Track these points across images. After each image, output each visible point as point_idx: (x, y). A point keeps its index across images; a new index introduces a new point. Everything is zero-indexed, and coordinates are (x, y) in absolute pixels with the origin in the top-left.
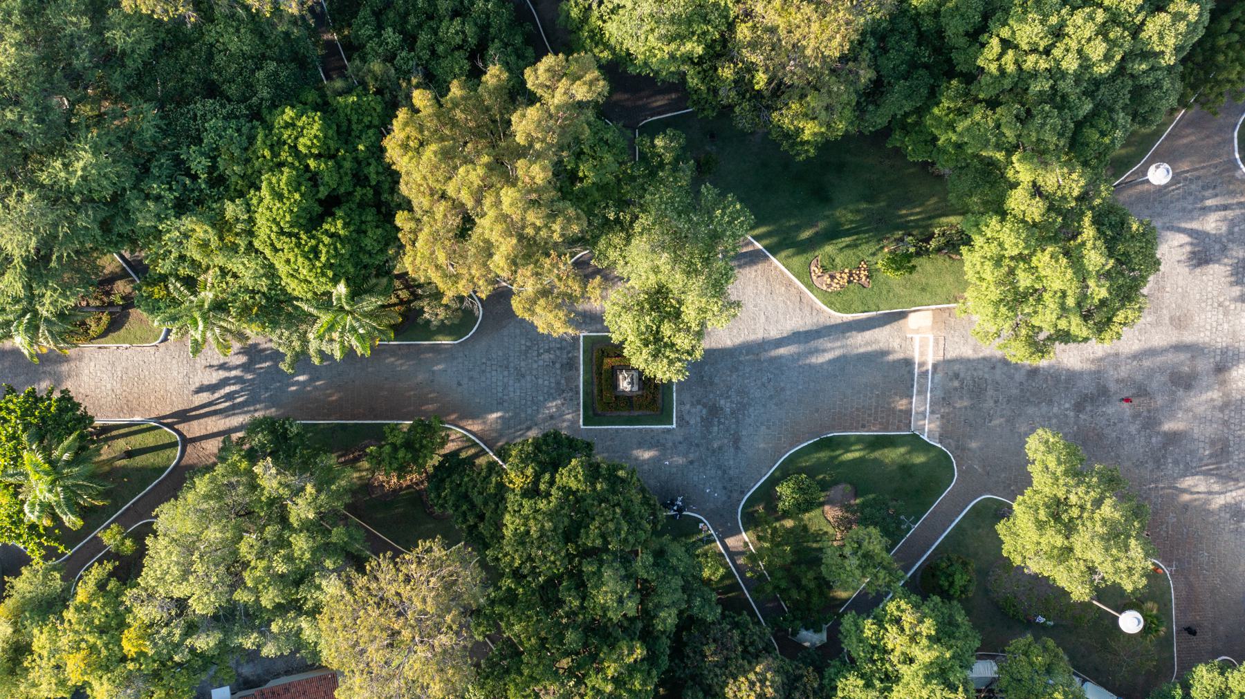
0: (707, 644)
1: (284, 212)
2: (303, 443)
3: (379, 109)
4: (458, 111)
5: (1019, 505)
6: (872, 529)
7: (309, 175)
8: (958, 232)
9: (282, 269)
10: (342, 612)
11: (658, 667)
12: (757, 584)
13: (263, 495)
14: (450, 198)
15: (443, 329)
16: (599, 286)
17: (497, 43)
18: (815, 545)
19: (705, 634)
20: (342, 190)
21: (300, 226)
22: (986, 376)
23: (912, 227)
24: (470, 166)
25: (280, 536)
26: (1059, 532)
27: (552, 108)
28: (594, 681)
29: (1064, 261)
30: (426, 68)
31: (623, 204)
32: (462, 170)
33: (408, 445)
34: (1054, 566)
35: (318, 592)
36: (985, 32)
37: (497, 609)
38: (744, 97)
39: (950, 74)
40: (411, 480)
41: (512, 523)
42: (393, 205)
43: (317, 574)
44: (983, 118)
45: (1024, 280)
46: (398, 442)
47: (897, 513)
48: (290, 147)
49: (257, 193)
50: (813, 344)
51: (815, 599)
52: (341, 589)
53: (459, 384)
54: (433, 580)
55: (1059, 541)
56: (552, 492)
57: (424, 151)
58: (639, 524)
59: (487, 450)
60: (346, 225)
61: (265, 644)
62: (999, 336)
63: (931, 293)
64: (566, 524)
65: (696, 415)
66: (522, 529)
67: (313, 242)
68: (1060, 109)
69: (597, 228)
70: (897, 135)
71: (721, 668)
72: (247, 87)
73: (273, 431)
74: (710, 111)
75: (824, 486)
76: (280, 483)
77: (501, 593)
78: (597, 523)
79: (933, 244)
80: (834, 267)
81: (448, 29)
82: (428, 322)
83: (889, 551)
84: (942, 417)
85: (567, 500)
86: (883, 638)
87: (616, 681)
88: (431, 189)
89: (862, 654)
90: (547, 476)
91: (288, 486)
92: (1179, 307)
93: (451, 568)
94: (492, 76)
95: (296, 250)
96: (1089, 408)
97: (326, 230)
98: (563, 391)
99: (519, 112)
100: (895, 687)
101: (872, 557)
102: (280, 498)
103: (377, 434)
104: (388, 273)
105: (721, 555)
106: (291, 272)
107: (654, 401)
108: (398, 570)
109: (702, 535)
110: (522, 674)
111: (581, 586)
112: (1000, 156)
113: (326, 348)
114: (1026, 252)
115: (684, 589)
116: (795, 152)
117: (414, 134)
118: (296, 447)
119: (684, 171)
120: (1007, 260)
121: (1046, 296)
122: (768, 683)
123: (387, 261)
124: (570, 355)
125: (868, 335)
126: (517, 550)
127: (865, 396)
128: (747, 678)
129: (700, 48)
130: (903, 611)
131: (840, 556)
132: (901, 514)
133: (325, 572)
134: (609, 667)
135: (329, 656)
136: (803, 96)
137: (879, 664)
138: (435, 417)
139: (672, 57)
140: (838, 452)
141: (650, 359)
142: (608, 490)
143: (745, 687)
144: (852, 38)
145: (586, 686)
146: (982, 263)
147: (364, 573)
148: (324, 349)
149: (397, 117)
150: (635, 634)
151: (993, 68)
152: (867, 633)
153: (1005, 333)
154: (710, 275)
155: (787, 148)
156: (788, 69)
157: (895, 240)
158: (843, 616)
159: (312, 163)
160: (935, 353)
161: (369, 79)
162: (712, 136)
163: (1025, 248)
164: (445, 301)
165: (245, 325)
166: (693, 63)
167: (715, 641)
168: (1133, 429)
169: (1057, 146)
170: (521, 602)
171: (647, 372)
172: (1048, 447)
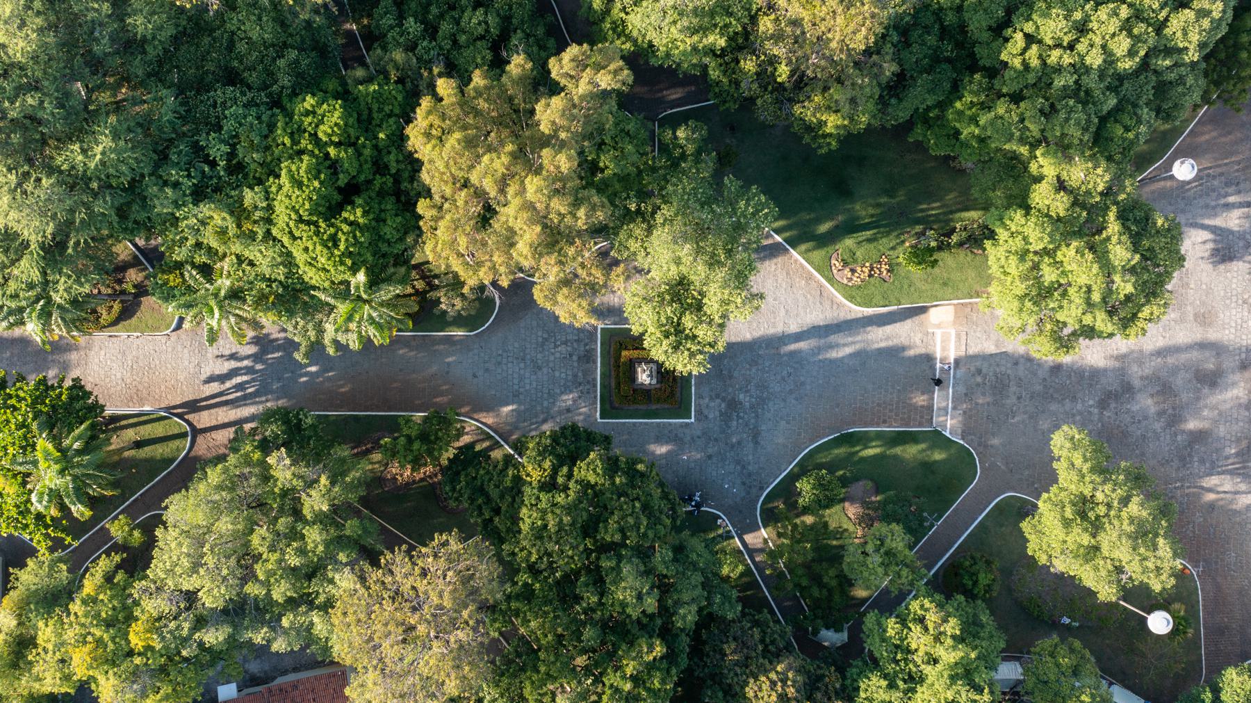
0: (727, 642)
1: (304, 199)
2: (316, 434)
3: (400, 98)
4: (481, 101)
5: (1045, 502)
6: (894, 526)
7: (329, 162)
8: (979, 226)
9: (300, 257)
10: (356, 608)
11: (677, 665)
12: (776, 580)
13: (276, 486)
14: (473, 185)
15: (459, 321)
16: (623, 274)
17: (519, 34)
18: (835, 543)
19: (725, 632)
20: (362, 178)
21: (320, 214)
22: (1009, 372)
23: (933, 222)
24: (494, 155)
25: (293, 528)
26: (1086, 530)
27: (575, 97)
28: (612, 679)
29: (1089, 256)
30: (447, 58)
31: (643, 195)
32: (486, 159)
33: (424, 437)
34: (1081, 565)
35: (330, 586)
36: (1009, 27)
37: (514, 605)
38: (766, 90)
39: (973, 67)
40: (425, 473)
41: (530, 517)
42: (412, 193)
43: (330, 567)
44: (1006, 112)
45: (1049, 275)
46: (413, 434)
47: (920, 510)
48: (310, 135)
49: (277, 181)
50: (833, 338)
51: (837, 598)
52: (355, 583)
53: (475, 376)
54: (450, 574)
55: (1086, 540)
56: (570, 486)
57: (447, 140)
58: (659, 519)
59: (502, 443)
60: (365, 213)
61: (275, 639)
62: (1024, 331)
63: (953, 288)
64: (585, 518)
65: (714, 409)
66: (539, 523)
67: (332, 230)
68: (1085, 103)
69: (618, 219)
70: (919, 129)
71: (741, 667)
72: (268, 75)
73: (286, 422)
74: (731, 104)
75: (844, 482)
76: (294, 474)
77: (517, 588)
78: (616, 518)
79: (955, 239)
80: (855, 261)
81: (470, 19)
82: (445, 313)
83: (911, 548)
84: (965, 412)
85: (585, 493)
86: (907, 638)
87: (635, 679)
88: (454, 178)
89: (885, 654)
90: (565, 470)
91: (301, 477)
92: (1203, 303)
93: (468, 563)
94: (517, 66)
95: (314, 238)
96: (1113, 405)
97: (345, 218)
98: (580, 384)
99: (543, 101)
100: (919, 688)
101: (894, 555)
102: (294, 489)
103: (392, 426)
104: (406, 262)
105: (740, 552)
106: (309, 260)
107: (672, 394)
108: (414, 564)
109: (720, 531)
110: (538, 672)
111: (599, 582)
112: (1024, 150)
113: (341, 338)
114: (1051, 246)
115: (704, 586)
116: (816, 145)
117: (437, 122)
118: (310, 438)
119: (706, 163)
120: (1031, 255)
121: (1071, 291)
122: (789, 683)
123: (406, 250)
124: (587, 347)
125: (888, 329)
126: (535, 545)
127: (886, 391)
128: (768, 678)
129: (723, 40)
130: (927, 610)
131: (862, 553)
132: (923, 511)
133: (338, 566)
134: (627, 665)
135: (340, 651)
136: (826, 89)
137: (902, 664)
138: (451, 409)
139: (695, 49)
140: (858, 448)
141: (670, 351)
142: (627, 484)
143: (766, 686)
144: (877, 31)
145: (604, 685)
146: (1007, 258)
147: (379, 567)
148: (339, 339)
149: (420, 105)
150: (654, 631)
151: (1017, 63)
152: (891, 632)
153: (1029, 328)
154: (734, 267)
155: (808, 141)
156: (810, 62)
157: (916, 233)
158: (865, 615)
159: (332, 151)
160: (957, 348)
161: (390, 68)
162: (732, 129)
163: (1050, 242)
164: (466, 290)
165: (261, 314)
166: (715, 55)
167: (735, 639)
168: (1158, 426)
169: (1081, 140)
170: (538, 597)
171: (667, 364)
172: (1074, 443)
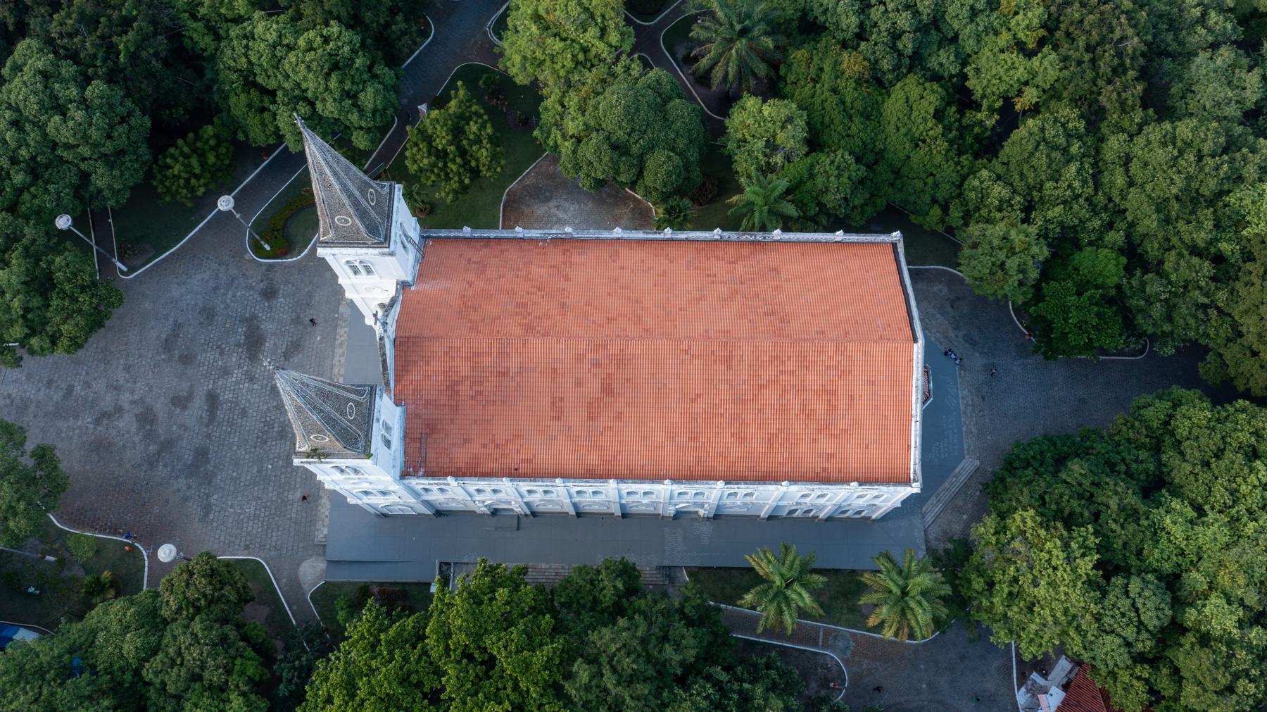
168: (137, 439)
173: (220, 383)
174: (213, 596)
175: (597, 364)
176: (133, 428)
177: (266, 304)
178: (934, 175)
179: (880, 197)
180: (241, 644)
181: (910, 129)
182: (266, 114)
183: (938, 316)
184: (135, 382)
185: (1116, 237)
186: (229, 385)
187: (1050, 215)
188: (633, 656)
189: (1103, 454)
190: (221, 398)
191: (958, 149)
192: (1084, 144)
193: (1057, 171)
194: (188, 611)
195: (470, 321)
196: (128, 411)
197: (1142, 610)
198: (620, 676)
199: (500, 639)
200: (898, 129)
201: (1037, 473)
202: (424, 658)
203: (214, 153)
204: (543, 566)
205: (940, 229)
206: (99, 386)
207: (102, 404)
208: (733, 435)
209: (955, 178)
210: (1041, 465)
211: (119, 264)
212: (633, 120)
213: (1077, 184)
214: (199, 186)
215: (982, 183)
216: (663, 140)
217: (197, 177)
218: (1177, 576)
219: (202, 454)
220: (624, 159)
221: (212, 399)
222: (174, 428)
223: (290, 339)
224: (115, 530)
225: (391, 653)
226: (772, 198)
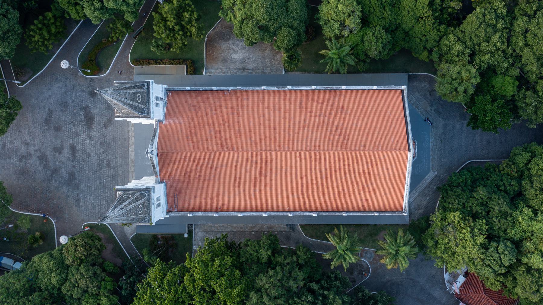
96: (24, 161)
168: (40, 168)
173: (75, 140)
174: (87, 254)
175: (256, 163)
176: (38, 163)
177: (92, 100)
178: (426, 36)
179: (398, 46)
180: (103, 275)
181: (415, 12)
182: (78, 7)
183: (423, 99)
184: (34, 141)
185: (515, 72)
186: (80, 141)
187: (483, 59)
188: (276, 288)
189: (495, 181)
190: (77, 148)
191: (439, 22)
192: (505, 21)
193: (489, 37)
194: (77, 261)
195: (193, 142)
196: (34, 155)
197: (503, 259)
198: (271, 297)
199: (217, 283)
200: (409, 12)
201: (463, 190)
202: (184, 291)
203: (54, 26)
204: (235, 225)
205: (427, 60)
206: (18, 143)
207: (21, 151)
208: (320, 192)
209: (437, 38)
210: (465, 186)
211: (16, 82)
212: (270, 14)
213: (498, 44)
214: (50, 44)
215: (450, 42)
216: (286, 23)
217: (46, 39)
218: (521, 241)
219: (72, 175)
220: (266, 34)
221: (73, 148)
222: (57, 163)
223: (106, 118)
224: (38, 211)
225: (169, 288)
226: (342, 55)
